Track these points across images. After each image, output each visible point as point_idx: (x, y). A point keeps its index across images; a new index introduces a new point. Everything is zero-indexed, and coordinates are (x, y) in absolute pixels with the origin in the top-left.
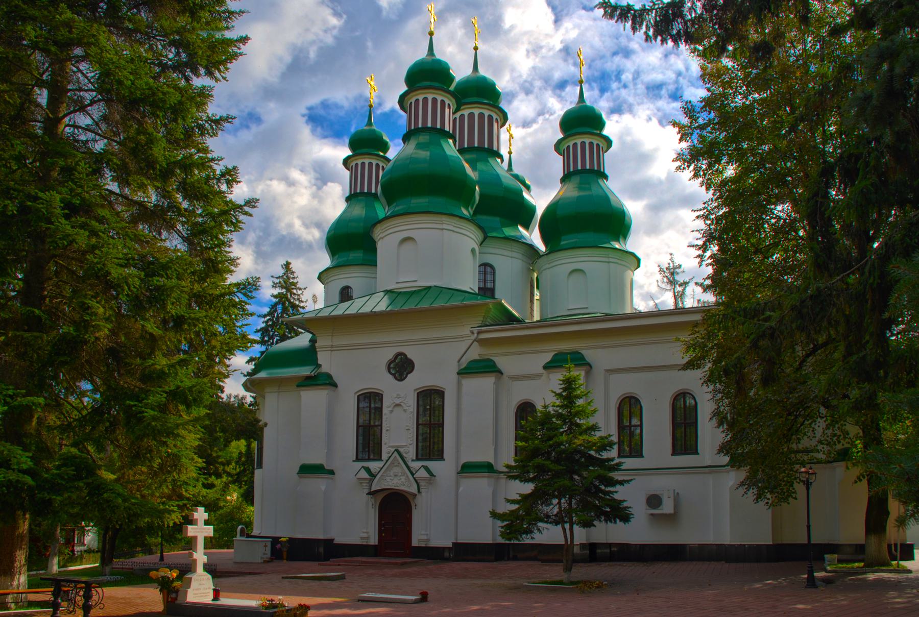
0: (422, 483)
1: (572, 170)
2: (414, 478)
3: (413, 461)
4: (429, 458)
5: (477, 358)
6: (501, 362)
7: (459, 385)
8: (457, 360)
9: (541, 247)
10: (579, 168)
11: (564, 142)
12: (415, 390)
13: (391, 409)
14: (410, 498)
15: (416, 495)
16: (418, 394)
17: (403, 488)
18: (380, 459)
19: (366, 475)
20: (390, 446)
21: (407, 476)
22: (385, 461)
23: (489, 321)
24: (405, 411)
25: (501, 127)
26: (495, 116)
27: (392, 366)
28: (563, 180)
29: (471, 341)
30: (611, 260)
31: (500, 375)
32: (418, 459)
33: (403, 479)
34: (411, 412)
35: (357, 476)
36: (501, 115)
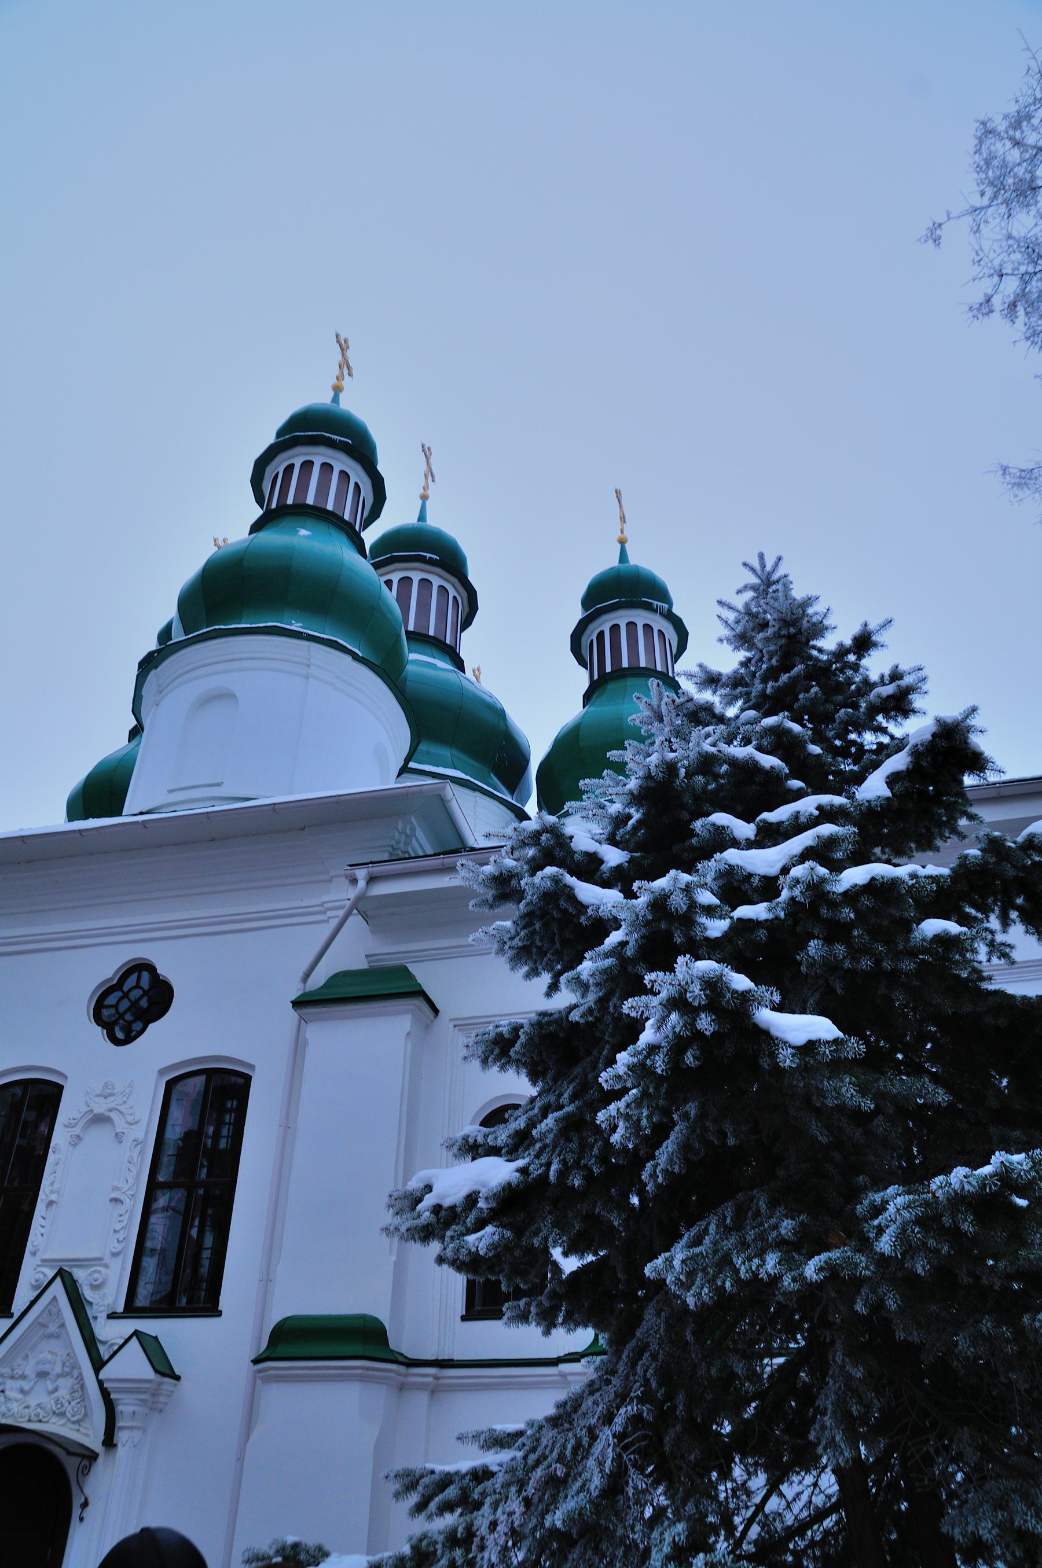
0: (125, 1407)
1: (608, 669)
3: (113, 1316)
5: (362, 964)
7: (299, 1047)
8: (300, 974)
11: (591, 626)
12: (162, 1072)
13: (77, 1131)
14: (71, 1465)
17: (54, 1426)
21: (80, 1378)
24: (119, 1137)
25: (462, 630)
26: (452, 592)
27: (111, 1000)
32: (131, 1310)
33: (65, 1385)
34: (137, 1142)
36: (465, 594)
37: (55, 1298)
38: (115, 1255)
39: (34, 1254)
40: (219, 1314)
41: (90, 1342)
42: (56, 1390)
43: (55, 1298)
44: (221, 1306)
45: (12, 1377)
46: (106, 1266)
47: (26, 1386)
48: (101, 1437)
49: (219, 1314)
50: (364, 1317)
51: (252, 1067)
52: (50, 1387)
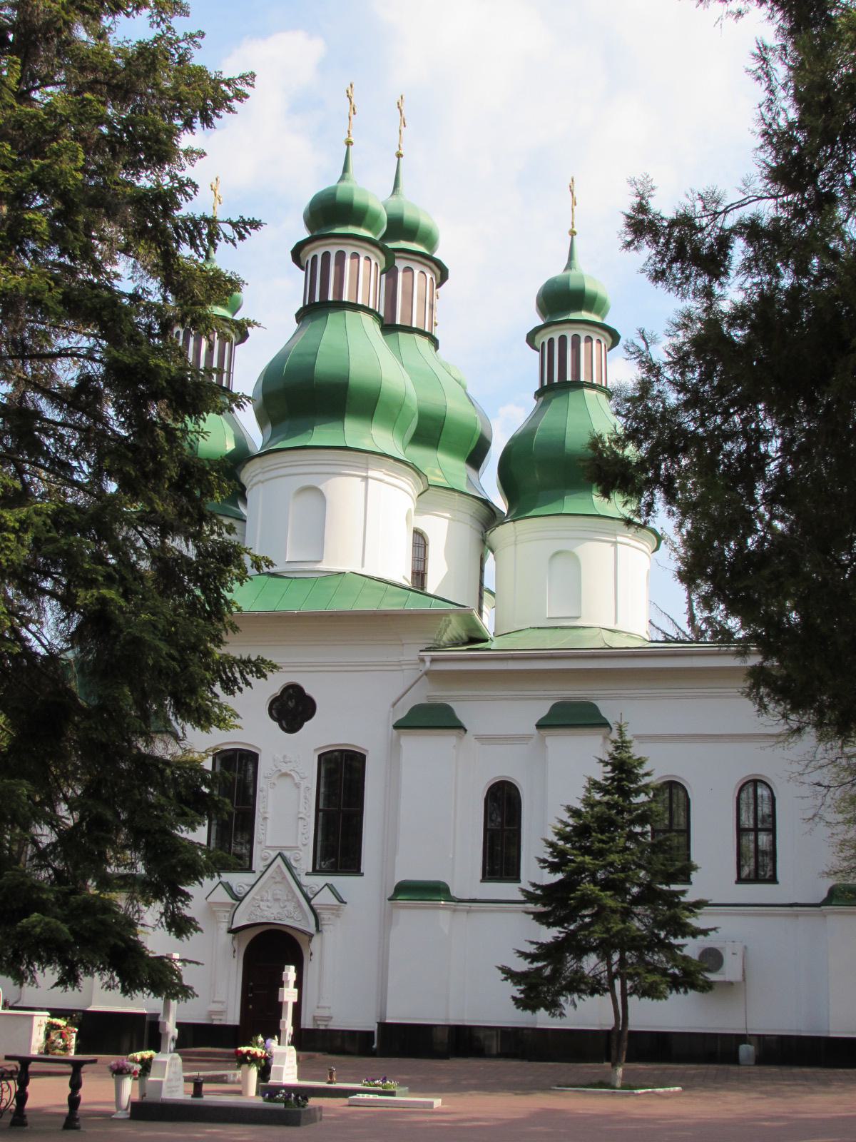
0: (325, 915)
1: (556, 380)
2: (311, 907)
3: (307, 874)
4: (336, 869)
5: (424, 701)
6: (462, 712)
7: (394, 749)
9: (501, 503)
10: (569, 378)
11: (543, 332)
12: (316, 750)
14: (301, 939)
15: (311, 936)
16: (320, 756)
18: (249, 869)
19: (227, 899)
20: (268, 847)
21: (298, 901)
22: (258, 874)
23: (445, 638)
24: (297, 786)
28: (539, 394)
29: (420, 674)
30: (619, 539)
31: (462, 732)
32: (316, 871)
33: (290, 906)
34: (308, 789)
35: (209, 899)
36: (438, 272)
37: (279, 866)
40: (362, 875)
41: (299, 885)
42: (285, 907)
43: (279, 866)
44: (362, 870)
45: (262, 900)
46: (300, 850)
47: (269, 904)
48: (315, 929)
49: (362, 875)
50: (439, 882)
51: (367, 751)
52: (282, 905)
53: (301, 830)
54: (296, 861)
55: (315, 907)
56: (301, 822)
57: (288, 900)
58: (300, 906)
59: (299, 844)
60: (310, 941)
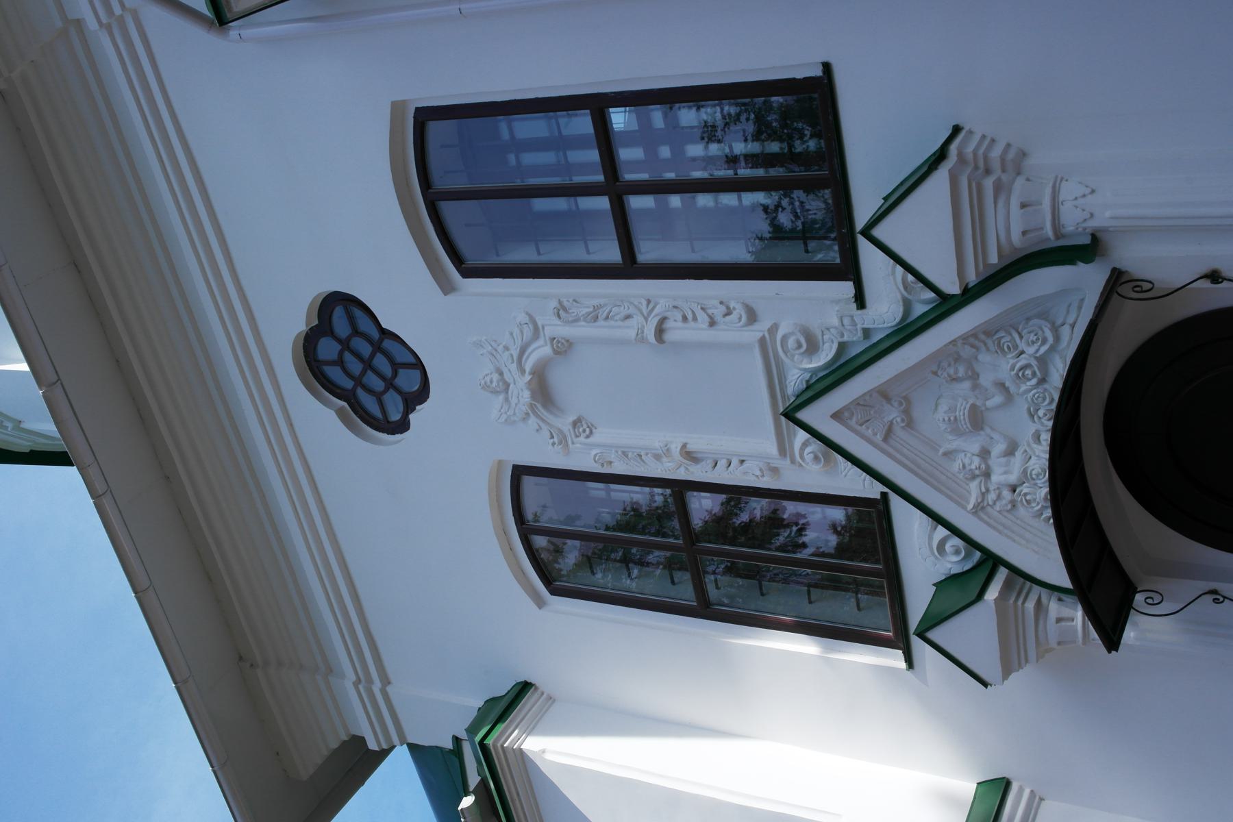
2: (970, 295)
12: (447, 287)
15: (1117, 278)
21: (971, 338)
24: (563, 348)
34: (561, 310)
37: (836, 416)
38: (752, 316)
39: (775, 471)
40: (827, 67)
41: (906, 332)
42: (1002, 386)
43: (836, 416)
45: (987, 475)
46: (773, 329)
47: (999, 448)
48: (1081, 268)
51: (397, 108)
52: (998, 399)
53: (698, 332)
54: (812, 347)
55: (972, 278)
56: (677, 332)
57: (974, 376)
58: (986, 334)
59: (752, 335)
60: (1136, 283)
